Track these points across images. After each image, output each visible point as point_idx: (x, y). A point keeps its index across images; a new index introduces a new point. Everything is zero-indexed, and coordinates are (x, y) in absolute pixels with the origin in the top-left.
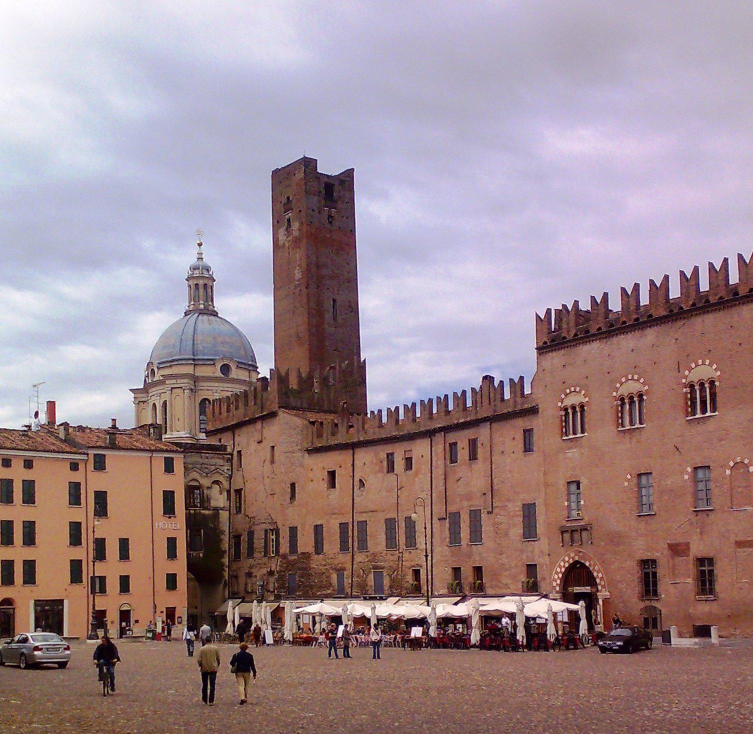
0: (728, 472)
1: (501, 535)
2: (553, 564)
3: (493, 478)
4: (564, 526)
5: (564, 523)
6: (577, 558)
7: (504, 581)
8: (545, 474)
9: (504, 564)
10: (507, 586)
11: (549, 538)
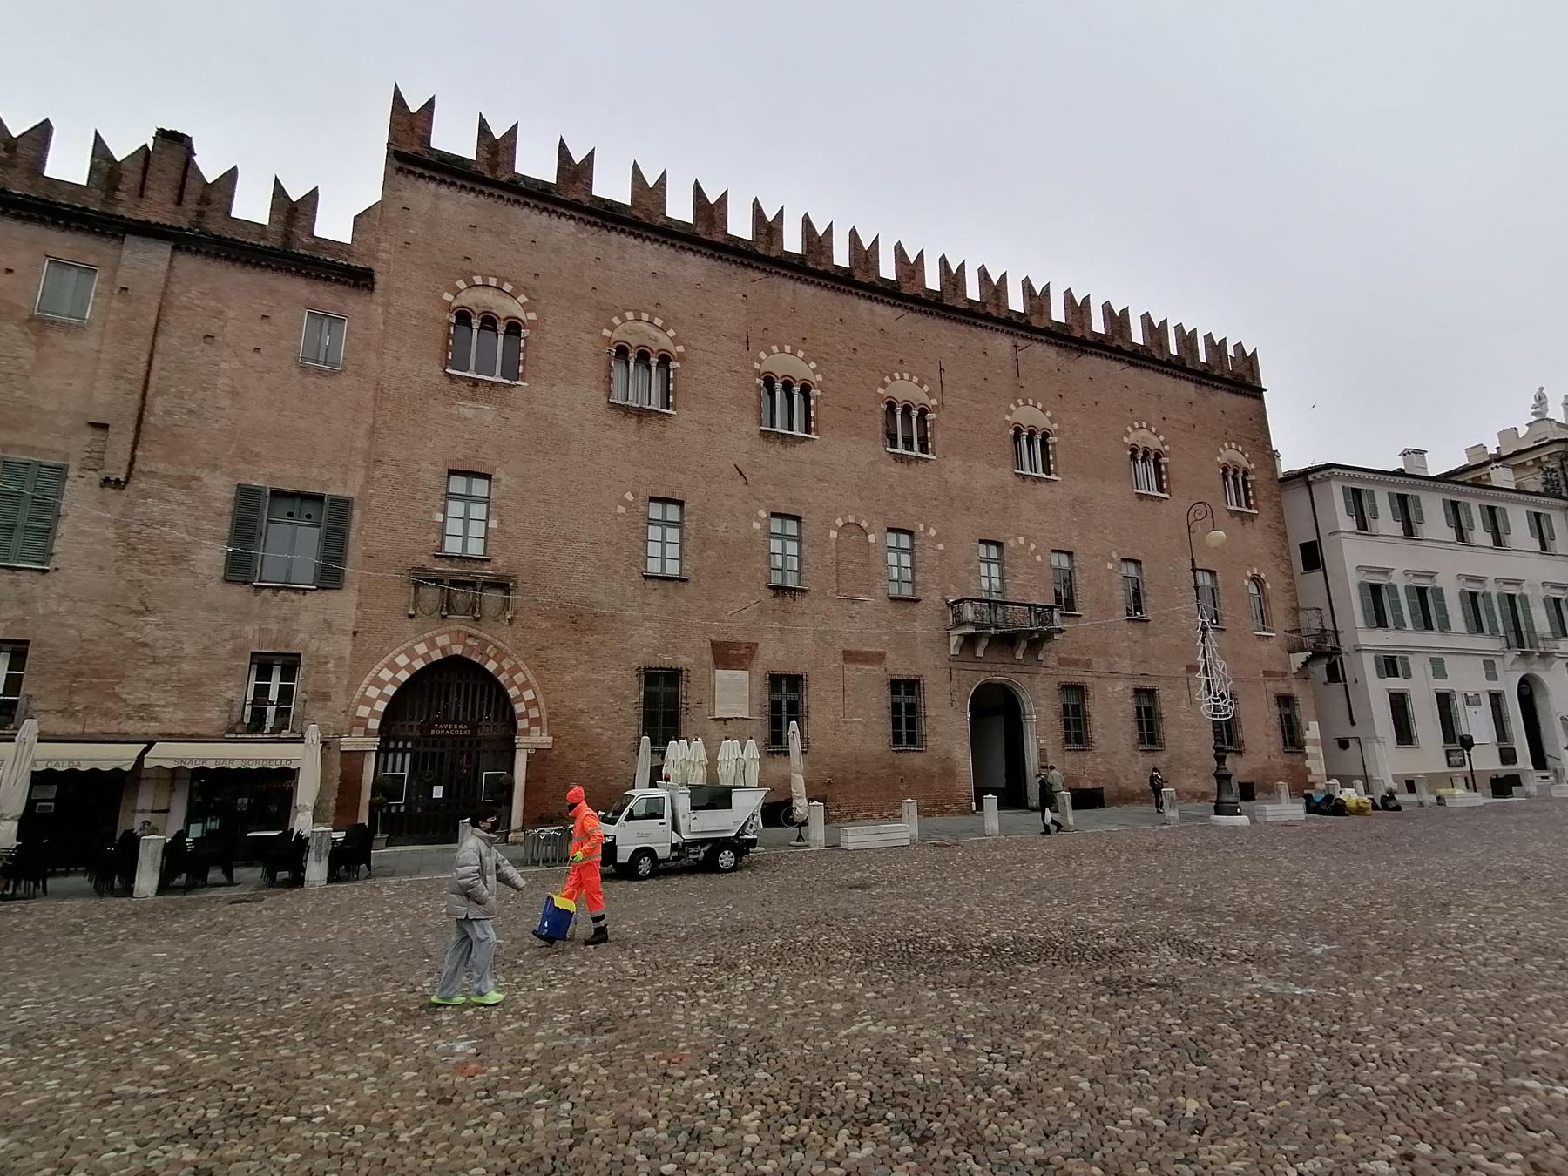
0: (833, 534)
1: (149, 557)
2: (363, 660)
3: (151, 390)
4: (423, 569)
5: (425, 561)
6: (458, 650)
7: (134, 694)
8: (373, 431)
9: (145, 645)
10: (144, 711)
11: (359, 591)
